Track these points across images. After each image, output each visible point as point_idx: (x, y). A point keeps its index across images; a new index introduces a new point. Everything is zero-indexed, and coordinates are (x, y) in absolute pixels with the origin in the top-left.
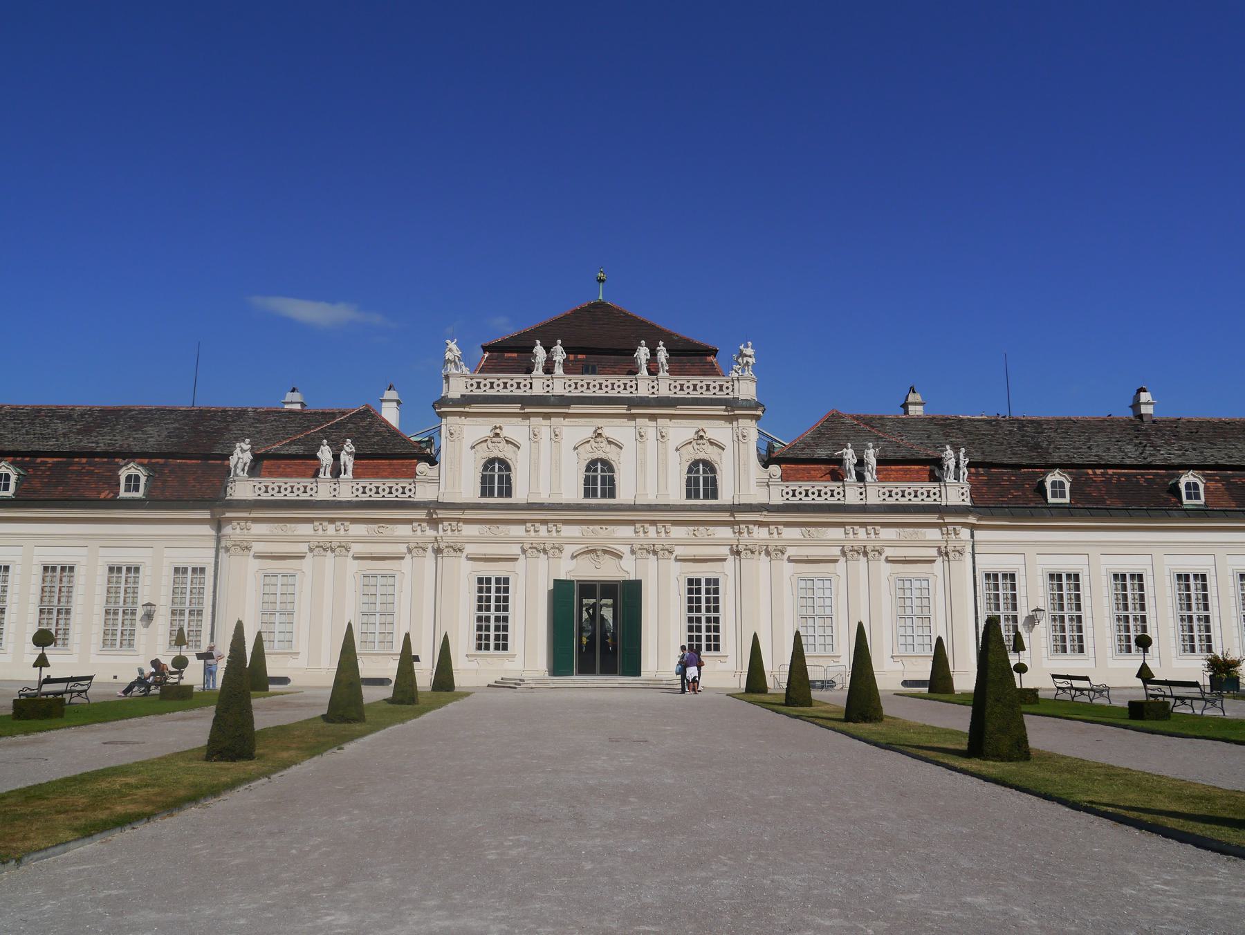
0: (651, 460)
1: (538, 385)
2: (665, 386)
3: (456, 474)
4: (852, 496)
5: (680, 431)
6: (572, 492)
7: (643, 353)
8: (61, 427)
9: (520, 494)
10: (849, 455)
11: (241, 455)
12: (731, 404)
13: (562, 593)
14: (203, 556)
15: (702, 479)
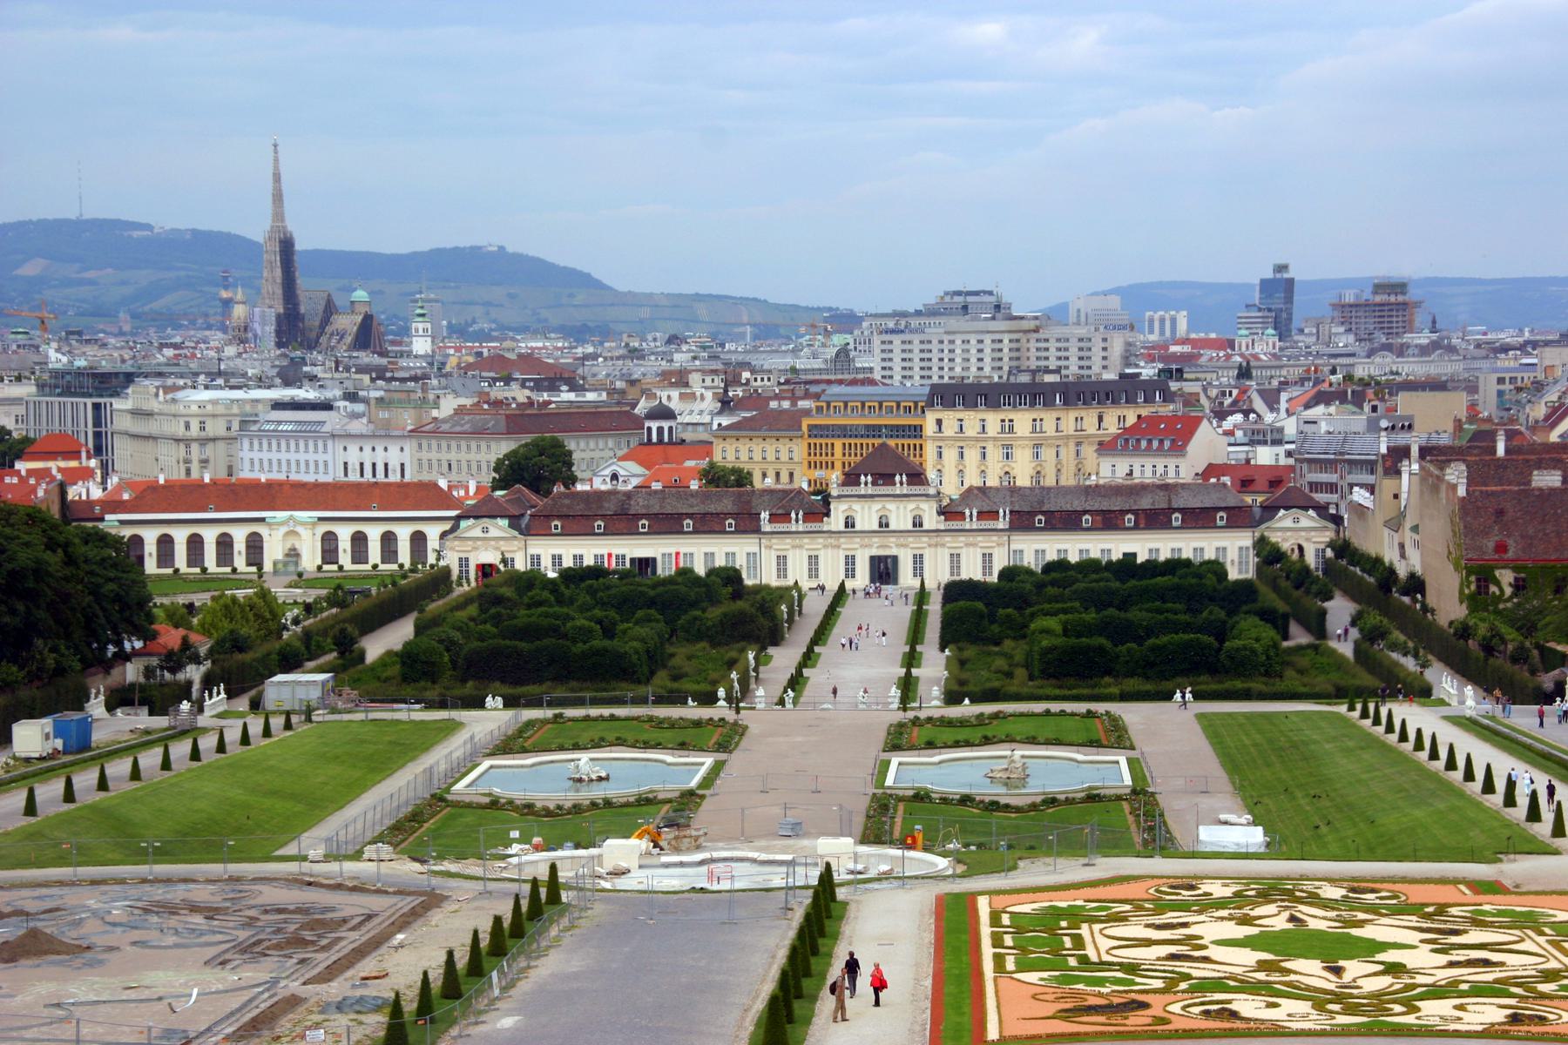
0: (901, 516)
1: (862, 490)
2: (905, 490)
3: (836, 521)
4: (968, 527)
5: (911, 506)
6: (875, 527)
7: (898, 478)
8: (693, 500)
9: (858, 527)
10: (967, 512)
11: (765, 515)
12: (927, 495)
13: (872, 558)
14: (755, 549)
15: (918, 522)
